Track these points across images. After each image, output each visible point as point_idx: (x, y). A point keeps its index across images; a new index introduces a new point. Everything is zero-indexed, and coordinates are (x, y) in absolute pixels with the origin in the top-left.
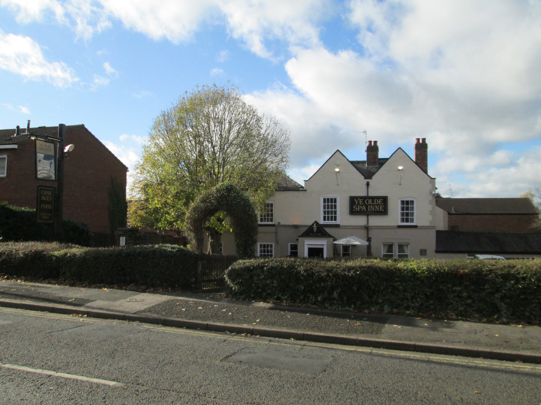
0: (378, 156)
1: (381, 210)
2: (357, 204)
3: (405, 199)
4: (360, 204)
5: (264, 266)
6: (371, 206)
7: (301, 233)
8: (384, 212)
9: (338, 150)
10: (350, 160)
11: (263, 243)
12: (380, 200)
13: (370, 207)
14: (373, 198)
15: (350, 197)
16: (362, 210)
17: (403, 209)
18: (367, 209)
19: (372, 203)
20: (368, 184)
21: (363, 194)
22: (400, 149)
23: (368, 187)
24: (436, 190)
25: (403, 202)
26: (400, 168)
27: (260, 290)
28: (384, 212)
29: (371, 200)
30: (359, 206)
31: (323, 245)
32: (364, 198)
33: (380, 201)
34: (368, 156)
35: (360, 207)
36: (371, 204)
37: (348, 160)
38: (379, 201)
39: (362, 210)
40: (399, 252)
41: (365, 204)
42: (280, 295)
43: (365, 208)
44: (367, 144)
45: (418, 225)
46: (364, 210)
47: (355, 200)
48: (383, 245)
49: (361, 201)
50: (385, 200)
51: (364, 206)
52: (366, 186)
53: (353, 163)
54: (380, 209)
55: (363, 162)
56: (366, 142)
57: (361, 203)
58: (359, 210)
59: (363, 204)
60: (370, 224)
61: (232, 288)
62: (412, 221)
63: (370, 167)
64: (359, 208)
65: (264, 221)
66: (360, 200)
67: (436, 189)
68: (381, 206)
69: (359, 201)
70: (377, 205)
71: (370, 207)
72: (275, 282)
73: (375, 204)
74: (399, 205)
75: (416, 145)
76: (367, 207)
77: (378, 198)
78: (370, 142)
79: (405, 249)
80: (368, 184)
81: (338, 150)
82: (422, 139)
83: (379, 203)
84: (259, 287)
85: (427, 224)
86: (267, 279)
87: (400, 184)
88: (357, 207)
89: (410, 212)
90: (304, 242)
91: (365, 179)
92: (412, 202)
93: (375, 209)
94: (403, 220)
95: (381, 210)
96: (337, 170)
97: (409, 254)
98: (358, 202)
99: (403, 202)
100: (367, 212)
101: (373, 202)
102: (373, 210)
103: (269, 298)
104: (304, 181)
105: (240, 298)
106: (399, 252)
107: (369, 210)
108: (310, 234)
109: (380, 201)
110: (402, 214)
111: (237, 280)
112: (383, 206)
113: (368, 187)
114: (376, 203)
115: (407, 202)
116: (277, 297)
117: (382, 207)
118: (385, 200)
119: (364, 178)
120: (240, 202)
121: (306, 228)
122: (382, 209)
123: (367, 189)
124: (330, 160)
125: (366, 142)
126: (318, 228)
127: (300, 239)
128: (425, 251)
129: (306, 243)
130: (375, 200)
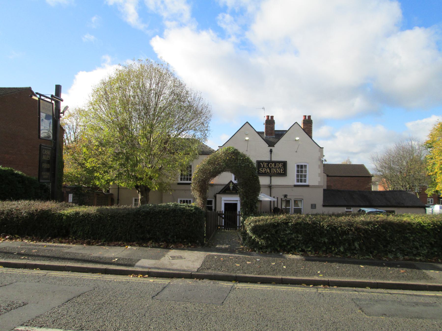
0: (274, 128)
1: (281, 172)
2: (262, 167)
4: (265, 167)
5: (288, 222)
6: (274, 169)
7: (219, 191)
8: (284, 174)
9: (247, 122)
10: (257, 131)
11: (183, 199)
12: (281, 164)
13: (273, 170)
14: (275, 162)
15: (257, 161)
16: (266, 172)
17: (298, 171)
18: (270, 171)
20: (271, 151)
21: (268, 159)
22: (296, 123)
23: (271, 154)
24: (324, 157)
25: (298, 166)
26: (297, 139)
27: (285, 243)
28: (284, 174)
29: (274, 164)
30: (264, 169)
31: (237, 201)
32: (268, 162)
33: (281, 165)
34: (266, 128)
35: (265, 169)
36: (274, 167)
37: (255, 130)
38: (280, 165)
39: (266, 172)
40: (294, 207)
41: (269, 167)
42: (304, 247)
43: (269, 170)
44: (266, 118)
45: (310, 184)
46: (268, 172)
47: (261, 163)
48: (271, 201)
49: (266, 164)
50: (284, 164)
51: (268, 169)
52: (270, 153)
53: (259, 133)
54: (280, 171)
55: (262, 133)
56: (265, 117)
57: (266, 166)
58: (264, 172)
59: (267, 167)
60: (273, 184)
61: (258, 242)
62: (305, 181)
63: (268, 137)
64: (264, 170)
65: (184, 180)
66: (265, 164)
67: (324, 156)
68: (281, 169)
69: (264, 164)
70: (279, 168)
71: (273, 170)
72: (300, 236)
73: (277, 167)
74: (296, 169)
75: (304, 120)
76: (270, 169)
77: (279, 162)
78: (268, 116)
79: (299, 204)
80: (271, 151)
81: (247, 122)
82: (308, 116)
83: (280, 166)
84: (283, 241)
85: (317, 184)
86: (292, 234)
87: (296, 152)
88: (263, 170)
89: (303, 174)
90: (221, 198)
91: (268, 146)
92: (305, 166)
94: (298, 181)
95: (281, 172)
96: (247, 138)
97: (302, 207)
98: (264, 166)
99: (298, 166)
101: (275, 165)
102: (276, 172)
103: (293, 250)
104: (219, 147)
105: (266, 251)
106: (294, 207)
107: (272, 172)
108: (227, 192)
109: (281, 165)
110: (298, 176)
111: (264, 235)
112: (283, 169)
113: (271, 154)
114: (278, 166)
115: (302, 166)
116: (302, 249)
117: (282, 170)
118: (284, 164)
119: (268, 145)
120: (248, 165)
121: (223, 187)
122: (282, 172)
123: (270, 155)
124: (240, 130)
125: (265, 117)
126: (233, 187)
127: (218, 196)
128: (312, 205)
130: (277, 164)
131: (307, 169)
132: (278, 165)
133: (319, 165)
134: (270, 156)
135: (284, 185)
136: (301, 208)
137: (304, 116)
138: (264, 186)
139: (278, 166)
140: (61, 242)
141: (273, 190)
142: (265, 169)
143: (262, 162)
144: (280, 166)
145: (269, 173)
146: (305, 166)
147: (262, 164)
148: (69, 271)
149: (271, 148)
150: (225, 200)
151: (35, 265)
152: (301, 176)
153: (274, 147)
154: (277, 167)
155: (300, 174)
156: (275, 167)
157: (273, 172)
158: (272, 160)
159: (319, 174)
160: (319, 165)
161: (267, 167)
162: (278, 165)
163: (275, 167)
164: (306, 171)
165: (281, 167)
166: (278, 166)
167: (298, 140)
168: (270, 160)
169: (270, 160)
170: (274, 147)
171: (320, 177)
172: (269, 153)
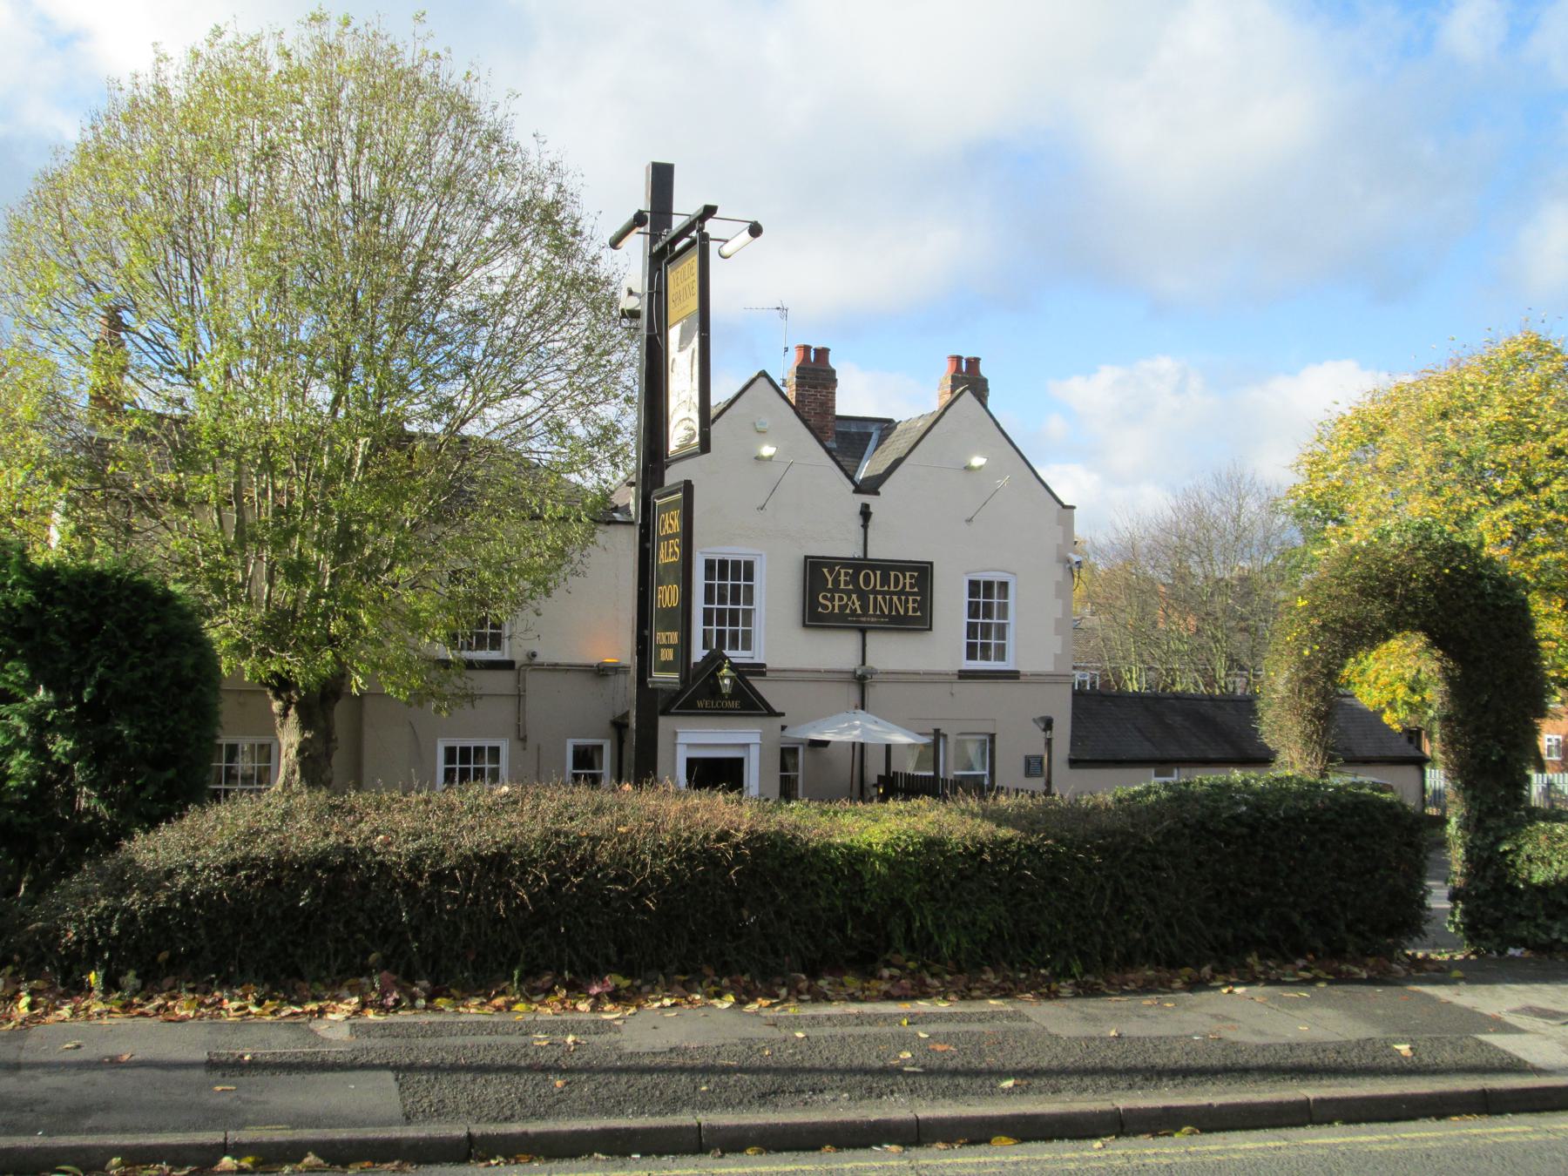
0: (834, 407)
2: (830, 586)
3: (982, 577)
4: (842, 586)
8: (918, 620)
9: (763, 374)
11: (459, 743)
13: (875, 600)
14: (886, 567)
15: (806, 557)
16: (848, 611)
17: (973, 611)
18: (864, 607)
19: (882, 586)
20: (866, 513)
21: (852, 550)
23: (865, 526)
25: (974, 585)
26: (977, 461)
28: (918, 620)
29: (878, 573)
30: (837, 595)
31: (747, 746)
32: (860, 565)
33: (908, 581)
35: (841, 599)
38: (905, 578)
39: (848, 611)
41: (858, 590)
43: (857, 604)
45: (1022, 669)
46: (854, 611)
47: (825, 570)
49: (846, 574)
50: (923, 572)
51: (854, 596)
52: (860, 521)
54: (906, 610)
57: (846, 583)
58: (836, 611)
59: (851, 587)
64: (837, 603)
66: (842, 571)
69: (839, 572)
70: (899, 594)
71: (875, 600)
73: (892, 589)
74: (965, 599)
76: (863, 597)
77: (903, 566)
80: (866, 513)
81: (763, 374)
83: (905, 584)
85: (1049, 667)
87: (969, 521)
88: (832, 600)
90: (676, 734)
91: (855, 492)
92: (1004, 586)
93: (890, 610)
94: (971, 655)
95: (910, 613)
98: (836, 582)
100: (864, 619)
101: (885, 580)
102: (886, 612)
107: (871, 612)
108: (700, 704)
109: (907, 580)
110: (972, 630)
113: (865, 526)
114: (895, 587)
115: (989, 585)
117: (914, 601)
118: (923, 572)
122: (914, 610)
123: (862, 530)
124: (733, 407)
129: (682, 739)
130: (892, 573)
131: (1011, 600)
132: (897, 577)
133: (1058, 583)
134: (862, 537)
135: (939, 674)
136: (983, 776)
137: (953, 357)
138: (825, 675)
139: (896, 585)
140: (819, 997)
141: (873, 693)
142: (841, 599)
143: (830, 562)
144: (905, 584)
145: (859, 616)
146: (1004, 586)
147: (831, 573)
148: (1330, 1122)
149: (866, 499)
150: (689, 745)
151: (1167, 1110)
152: (987, 628)
153: (877, 494)
154: (892, 589)
155: (981, 620)
156: (886, 588)
157: (875, 610)
158: (869, 556)
159: (1057, 620)
160: (1058, 583)
161: (851, 587)
162: (897, 579)
163: (886, 588)
164: (1004, 609)
165: (907, 589)
166: (896, 585)
167: (770, 458)
168: (862, 556)
169: (859, 554)
170: (877, 494)
171: (1059, 637)
172: (859, 521)
